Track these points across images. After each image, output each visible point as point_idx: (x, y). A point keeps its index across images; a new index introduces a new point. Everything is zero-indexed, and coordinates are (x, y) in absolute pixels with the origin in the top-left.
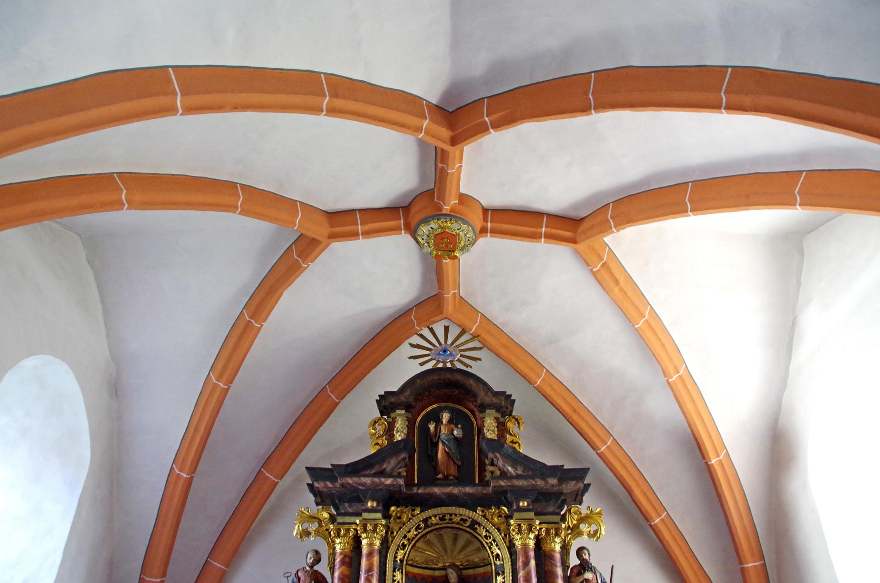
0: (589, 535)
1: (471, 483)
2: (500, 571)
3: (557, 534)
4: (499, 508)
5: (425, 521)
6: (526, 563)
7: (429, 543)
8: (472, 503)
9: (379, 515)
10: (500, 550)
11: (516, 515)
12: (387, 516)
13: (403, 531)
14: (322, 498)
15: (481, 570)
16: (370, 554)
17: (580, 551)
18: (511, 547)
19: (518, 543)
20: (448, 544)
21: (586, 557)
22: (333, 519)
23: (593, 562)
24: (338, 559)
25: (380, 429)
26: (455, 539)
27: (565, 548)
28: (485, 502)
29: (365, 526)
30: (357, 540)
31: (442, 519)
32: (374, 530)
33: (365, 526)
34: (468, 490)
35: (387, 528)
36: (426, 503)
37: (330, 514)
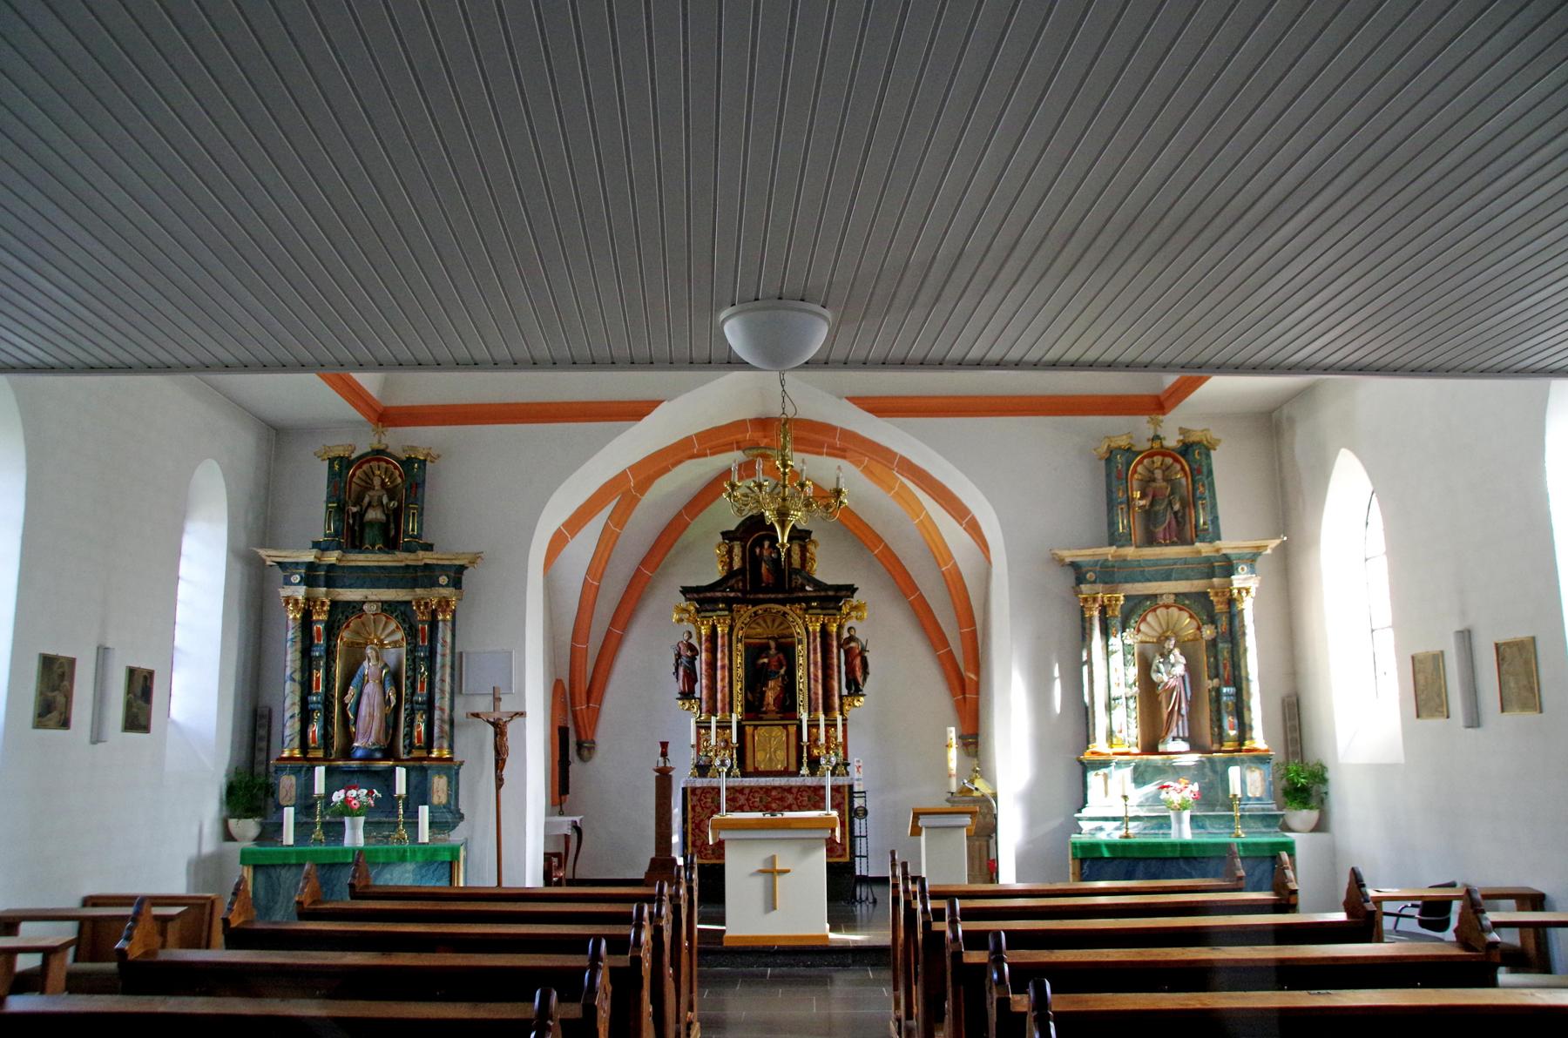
0: (857, 618)
1: (783, 591)
2: (800, 642)
3: (835, 622)
4: (800, 604)
5: (755, 613)
6: (815, 640)
7: (758, 624)
8: (783, 602)
9: (727, 613)
10: (799, 630)
11: (810, 611)
12: (731, 611)
13: (742, 619)
14: (687, 599)
15: (790, 640)
16: (723, 636)
17: (850, 629)
18: (807, 629)
19: (811, 629)
20: (770, 624)
21: (853, 633)
22: (698, 611)
23: (857, 636)
24: (703, 639)
25: (724, 550)
26: (774, 621)
27: (840, 627)
28: (792, 601)
29: (719, 620)
30: (714, 628)
31: (766, 610)
32: (724, 623)
33: (719, 620)
34: (780, 596)
35: (733, 619)
36: (755, 603)
37: (696, 608)
